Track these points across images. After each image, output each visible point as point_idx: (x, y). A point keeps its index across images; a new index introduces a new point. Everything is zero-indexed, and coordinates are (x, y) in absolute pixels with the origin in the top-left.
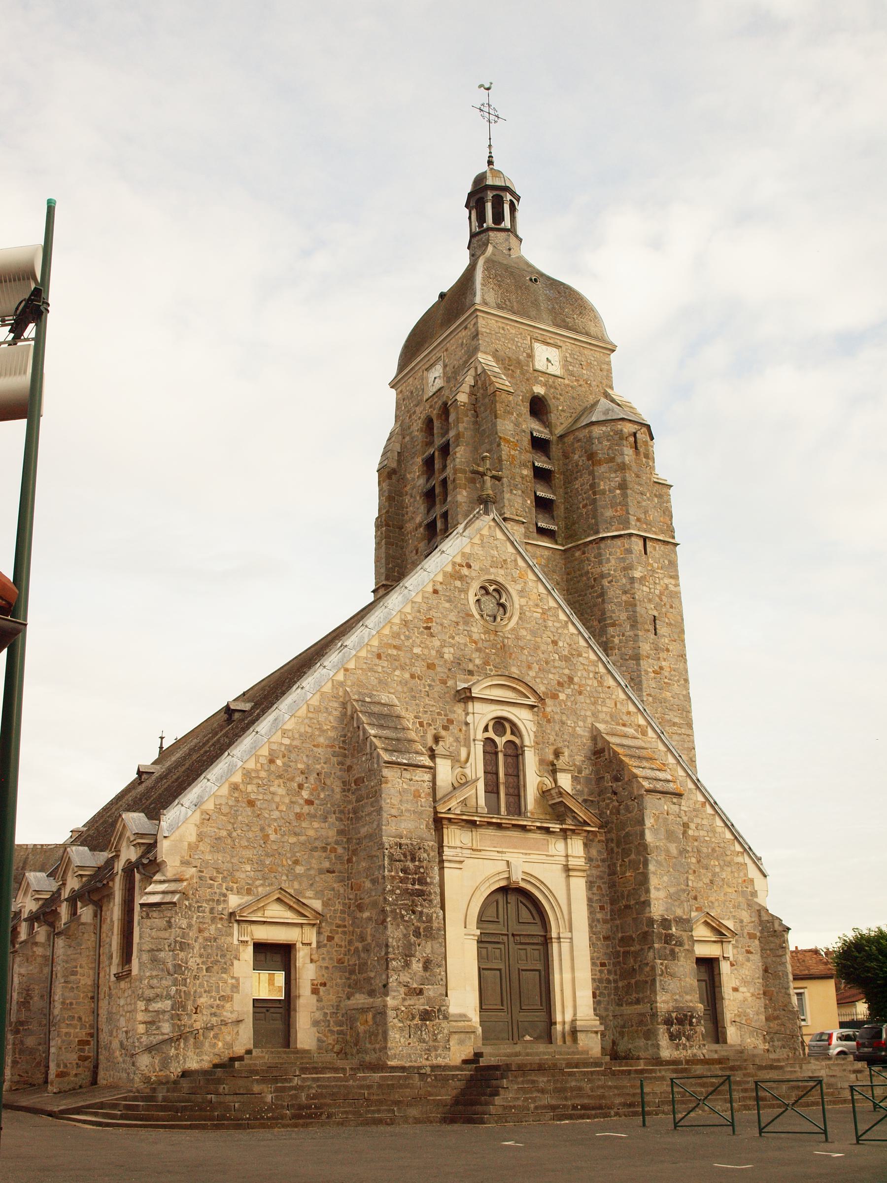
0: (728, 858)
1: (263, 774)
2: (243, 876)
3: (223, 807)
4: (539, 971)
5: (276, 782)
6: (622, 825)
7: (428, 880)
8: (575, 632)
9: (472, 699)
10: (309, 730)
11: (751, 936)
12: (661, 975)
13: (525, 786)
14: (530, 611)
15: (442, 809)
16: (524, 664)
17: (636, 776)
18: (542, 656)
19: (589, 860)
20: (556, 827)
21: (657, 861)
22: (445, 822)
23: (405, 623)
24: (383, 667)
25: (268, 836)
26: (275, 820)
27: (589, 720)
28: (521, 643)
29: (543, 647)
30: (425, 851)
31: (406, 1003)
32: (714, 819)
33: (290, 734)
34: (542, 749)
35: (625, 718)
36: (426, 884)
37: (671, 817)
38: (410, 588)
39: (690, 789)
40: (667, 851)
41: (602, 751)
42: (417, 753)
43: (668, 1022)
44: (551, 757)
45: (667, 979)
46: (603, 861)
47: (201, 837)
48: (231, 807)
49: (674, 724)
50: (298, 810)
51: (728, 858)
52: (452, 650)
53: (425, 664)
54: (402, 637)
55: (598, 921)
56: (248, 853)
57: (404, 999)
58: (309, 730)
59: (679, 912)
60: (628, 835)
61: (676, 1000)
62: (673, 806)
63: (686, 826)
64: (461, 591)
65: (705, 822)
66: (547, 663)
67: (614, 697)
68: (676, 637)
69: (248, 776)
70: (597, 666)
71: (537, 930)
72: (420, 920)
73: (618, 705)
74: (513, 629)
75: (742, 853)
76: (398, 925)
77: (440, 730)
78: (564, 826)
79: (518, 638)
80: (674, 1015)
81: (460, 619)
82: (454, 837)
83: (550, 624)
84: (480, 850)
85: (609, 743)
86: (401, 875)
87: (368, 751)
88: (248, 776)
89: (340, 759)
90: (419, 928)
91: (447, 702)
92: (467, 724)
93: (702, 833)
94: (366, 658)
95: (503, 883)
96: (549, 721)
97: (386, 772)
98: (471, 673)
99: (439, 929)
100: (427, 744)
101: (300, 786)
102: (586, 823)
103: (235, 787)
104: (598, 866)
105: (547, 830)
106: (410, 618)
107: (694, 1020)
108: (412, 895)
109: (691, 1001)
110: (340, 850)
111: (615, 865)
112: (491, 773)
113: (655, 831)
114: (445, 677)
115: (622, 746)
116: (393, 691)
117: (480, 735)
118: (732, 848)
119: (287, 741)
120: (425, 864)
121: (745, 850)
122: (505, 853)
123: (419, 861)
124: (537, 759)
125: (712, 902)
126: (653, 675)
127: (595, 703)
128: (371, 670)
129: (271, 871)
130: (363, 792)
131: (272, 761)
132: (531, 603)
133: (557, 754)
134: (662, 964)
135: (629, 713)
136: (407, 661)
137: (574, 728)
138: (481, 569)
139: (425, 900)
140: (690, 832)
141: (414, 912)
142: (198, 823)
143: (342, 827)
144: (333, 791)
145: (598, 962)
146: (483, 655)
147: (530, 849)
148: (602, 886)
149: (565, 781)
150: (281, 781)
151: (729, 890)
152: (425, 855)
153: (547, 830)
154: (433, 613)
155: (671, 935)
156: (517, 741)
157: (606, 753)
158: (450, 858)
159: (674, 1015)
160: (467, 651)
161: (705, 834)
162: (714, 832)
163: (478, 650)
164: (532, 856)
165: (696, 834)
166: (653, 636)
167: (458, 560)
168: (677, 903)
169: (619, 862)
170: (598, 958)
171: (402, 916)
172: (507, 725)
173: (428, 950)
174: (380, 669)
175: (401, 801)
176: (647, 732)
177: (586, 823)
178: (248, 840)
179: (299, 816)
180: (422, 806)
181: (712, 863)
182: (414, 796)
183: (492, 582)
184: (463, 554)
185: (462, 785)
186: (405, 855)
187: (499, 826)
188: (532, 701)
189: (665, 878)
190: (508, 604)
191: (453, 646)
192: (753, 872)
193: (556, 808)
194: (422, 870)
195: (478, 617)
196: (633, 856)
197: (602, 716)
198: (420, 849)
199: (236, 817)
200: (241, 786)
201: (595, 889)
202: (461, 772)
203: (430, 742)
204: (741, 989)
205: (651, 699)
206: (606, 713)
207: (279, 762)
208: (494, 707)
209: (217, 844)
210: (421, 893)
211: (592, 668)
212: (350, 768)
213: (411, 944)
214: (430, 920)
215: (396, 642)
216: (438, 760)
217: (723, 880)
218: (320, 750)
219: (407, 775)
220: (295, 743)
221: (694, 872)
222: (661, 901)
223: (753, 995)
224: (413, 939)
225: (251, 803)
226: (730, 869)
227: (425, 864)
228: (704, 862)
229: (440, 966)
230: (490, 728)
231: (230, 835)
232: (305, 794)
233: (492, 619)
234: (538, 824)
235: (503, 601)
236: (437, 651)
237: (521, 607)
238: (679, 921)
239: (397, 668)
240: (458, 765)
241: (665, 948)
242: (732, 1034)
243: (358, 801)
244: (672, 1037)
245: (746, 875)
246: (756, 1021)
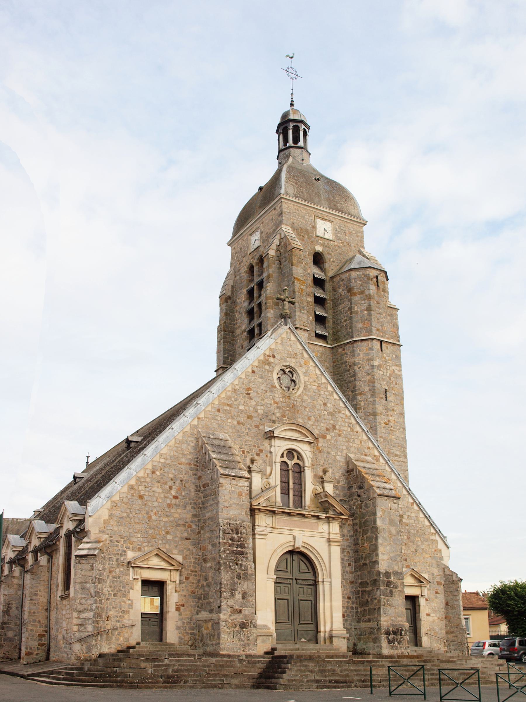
0: (426, 537)
1: (148, 480)
2: (136, 540)
3: (124, 499)
4: (311, 601)
5: (156, 485)
6: (363, 515)
7: (246, 545)
8: (338, 398)
9: (274, 437)
10: (176, 454)
11: (439, 583)
12: (384, 605)
13: (305, 490)
14: (310, 385)
15: (255, 503)
16: (306, 417)
17: (372, 486)
18: (317, 412)
19: (343, 535)
20: (323, 515)
21: (383, 537)
22: (256, 511)
23: (235, 391)
24: (221, 417)
25: (151, 517)
26: (155, 507)
27: (345, 452)
28: (304, 404)
29: (318, 407)
30: (244, 528)
31: (232, 618)
32: (419, 513)
33: (165, 456)
34: (316, 469)
35: (366, 451)
36: (245, 547)
37: (392, 511)
38: (238, 369)
39: (404, 495)
40: (390, 532)
41: (352, 470)
42: (241, 469)
44: (321, 474)
45: (388, 608)
46: (351, 536)
47: (111, 516)
48: (129, 499)
49: (396, 455)
50: (169, 501)
51: (426, 537)
52: (262, 407)
53: (246, 416)
54: (233, 399)
55: (347, 572)
56: (139, 527)
57: (230, 615)
58: (176, 454)
59: (396, 568)
60: (366, 521)
61: (392, 620)
62: (394, 505)
63: (401, 516)
64: (269, 372)
65: (413, 515)
66: (320, 416)
67: (360, 438)
68: (399, 402)
69: (139, 480)
70: (350, 419)
71: (310, 577)
72: (241, 569)
73: (363, 442)
74: (300, 396)
75: (435, 534)
76: (228, 572)
77: (255, 455)
78: (328, 515)
79: (303, 401)
80: (391, 629)
81: (268, 389)
82: (262, 520)
83: (322, 392)
84: (277, 529)
85: (356, 466)
86: (230, 542)
87: (211, 467)
88: (139, 480)
89: (194, 472)
90: (240, 574)
91: (259, 439)
92: (271, 452)
93: (411, 521)
94: (211, 411)
95: (290, 548)
96: (320, 452)
97: (222, 480)
98: (274, 422)
99: (252, 575)
100: (246, 464)
101: (171, 488)
102: (341, 514)
103: (132, 487)
104: (348, 540)
105: (318, 517)
106: (237, 387)
107: (403, 632)
108: (236, 554)
109: (401, 621)
110: (194, 526)
111: (358, 539)
112: (285, 482)
113: (383, 520)
114: (258, 424)
115: (364, 467)
116: (226, 432)
117: (279, 460)
118: (429, 531)
119: (163, 461)
120: (244, 535)
121: (437, 532)
122: (292, 530)
123: (241, 534)
124: (313, 475)
126: (384, 425)
127: (348, 442)
128: (213, 418)
129: (153, 537)
130: (208, 492)
131: (153, 472)
132: (311, 380)
133: (325, 472)
134: (384, 599)
135: (369, 448)
136: (236, 414)
137: (335, 456)
138: (281, 359)
139: (244, 557)
140: (404, 521)
141: (237, 564)
142: (109, 508)
143: (195, 513)
144: (190, 491)
145: (346, 597)
146: (281, 411)
147: (307, 528)
148: (350, 551)
149: (329, 488)
150: (159, 484)
151: (426, 556)
152: (244, 531)
153: (318, 517)
154: (251, 385)
156: (301, 463)
157: (354, 472)
158: (259, 533)
159: (391, 629)
160: (272, 409)
161: (413, 521)
162: (418, 520)
163: (278, 408)
164: (308, 533)
165: (407, 522)
166: (384, 401)
167: (268, 353)
168: (395, 563)
169: (361, 538)
170: (346, 594)
171: (230, 567)
172: (295, 454)
173: (245, 587)
174: (219, 418)
175: (230, 498)
176: (379, 459)
177: (341, 514)
178: (139, 519)
179: (169, 505)
180: (243, 501)
181: (417, 539)
182: (239, 495)
183: (288, 366)
184: (271, 349)
185: (267, 489)
186: (232, 531)
187: (289, 514)
188: (310, 439)
189: (388, 548)
190: (297, 380)
191: (263, 405)
192: (441, 545)
193: (324, 505)
194: (242, 539)
195: (279, 387)
196: (369, 534)
197: (352, 449)
198: (241, 527)
199: (132, 505)
200: (135, 487)
201: (345, 553)
202: (267, 482)
203: (248, 463)
204: (432, 615)
205: (382, 440)
206: (355, 447)
207: (158, 473)
208: (287, 442)
209: (121, 521)
210: (241, 553)
211: (347, 420)
212: (200, 477)
213: (235, 583)
214: (246, 569)
215: (230, 402)
216: (253, 474)
217: (423, 549)
218: (182, 466)
219: (234, 482)
220: (168, 462)
221: (406, 544)
222: (385, 561)
223: (438, 618)
224: (236, 580)
225: (141, 497)
226: (427, 543)
227: (244, 535)
228: (412, 538)
229: (252, 597)
230: (285, 455)
231: (128, 516)
232: (173, 492)
233: (287, 389)
234: (313, 514)
235: (294, 378)
236: (254, 408)
237: (305, 382)
238: (396, 573)
239: (229, 418)
240: (265, 477)
241: (387, 589)
242: (425, 641)
243: (204, 497)
244: (389, 642)
245: (437, 547)
246: (440, 634)
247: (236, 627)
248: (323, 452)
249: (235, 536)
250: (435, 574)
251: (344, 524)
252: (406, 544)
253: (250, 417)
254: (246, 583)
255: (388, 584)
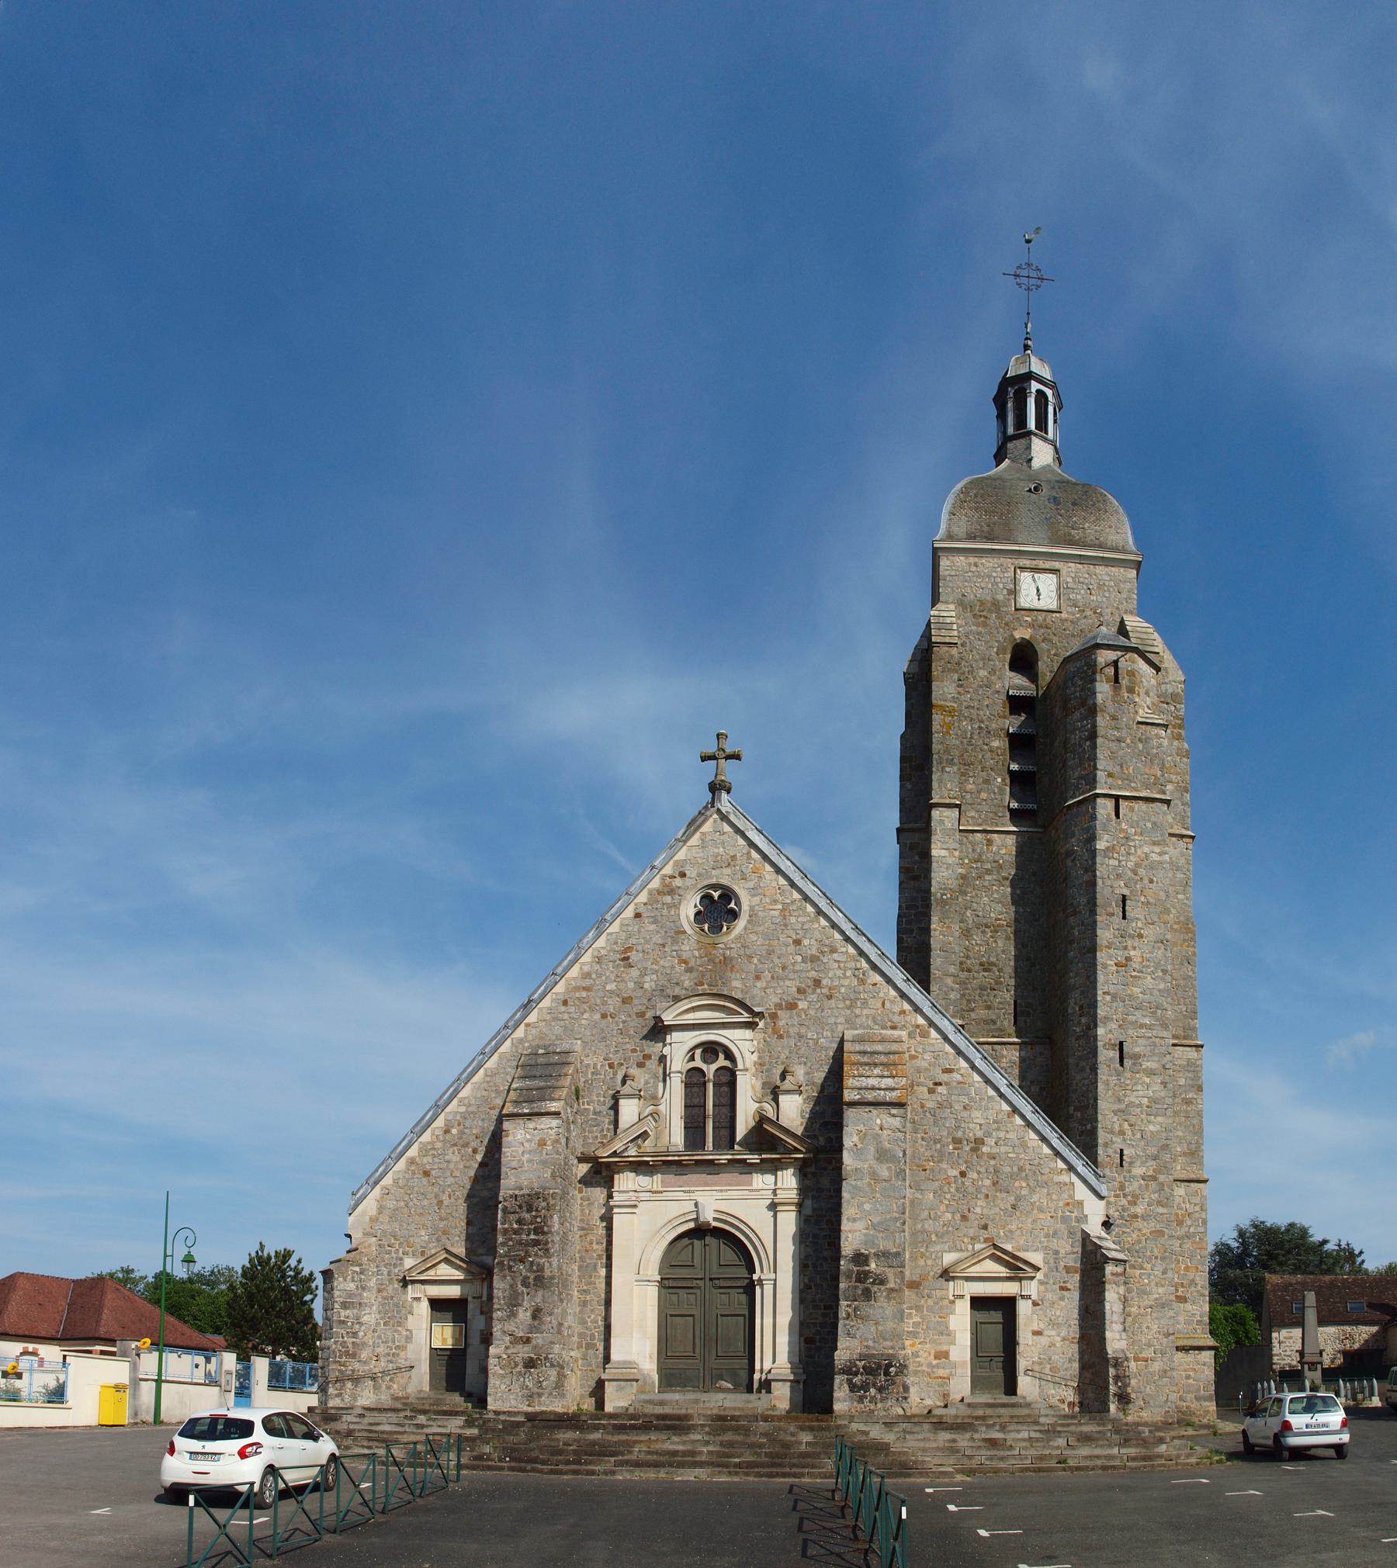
0: (1045, 1178)
16: (751, 976)
27: (840, 1028)
36: (544, 1233)
39: (990, 1098)
43: (849, 1370)
51: (1045, 1178)
55: (825, 1259)
59: (883, 1245)
65: (1011, 1135)
93: (1003, 1149)
96: (781, 1037)
114: (643, 1009)
118: (1052, 1165)
125: (1011, 1231)
145: (822, 1305)
155: (867, 1274)
163: (689, 970)
170: (821, 1300)
171: (510, 1267)
173: (538, 1299)
186: (520, 1207)
210: (536, 1243)
214: (541, 1269)
219: (531, 1125)
221: (987, 1196)
224: (520, 1288)
238: (883, 1255)
241: (856, 1287)
244: (853, 1388)
245: (1072, 1197)
247: (516, 1365)
248: (789, 1037)
249: (527, 1216)
250: (1063, 1251)
251: (825, 1169)
252: (987, 1196)
253: (627, 1001)
254: (540, 1293)
255: (862, 1277)
